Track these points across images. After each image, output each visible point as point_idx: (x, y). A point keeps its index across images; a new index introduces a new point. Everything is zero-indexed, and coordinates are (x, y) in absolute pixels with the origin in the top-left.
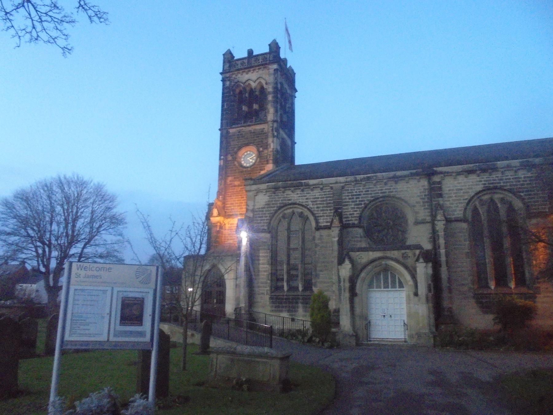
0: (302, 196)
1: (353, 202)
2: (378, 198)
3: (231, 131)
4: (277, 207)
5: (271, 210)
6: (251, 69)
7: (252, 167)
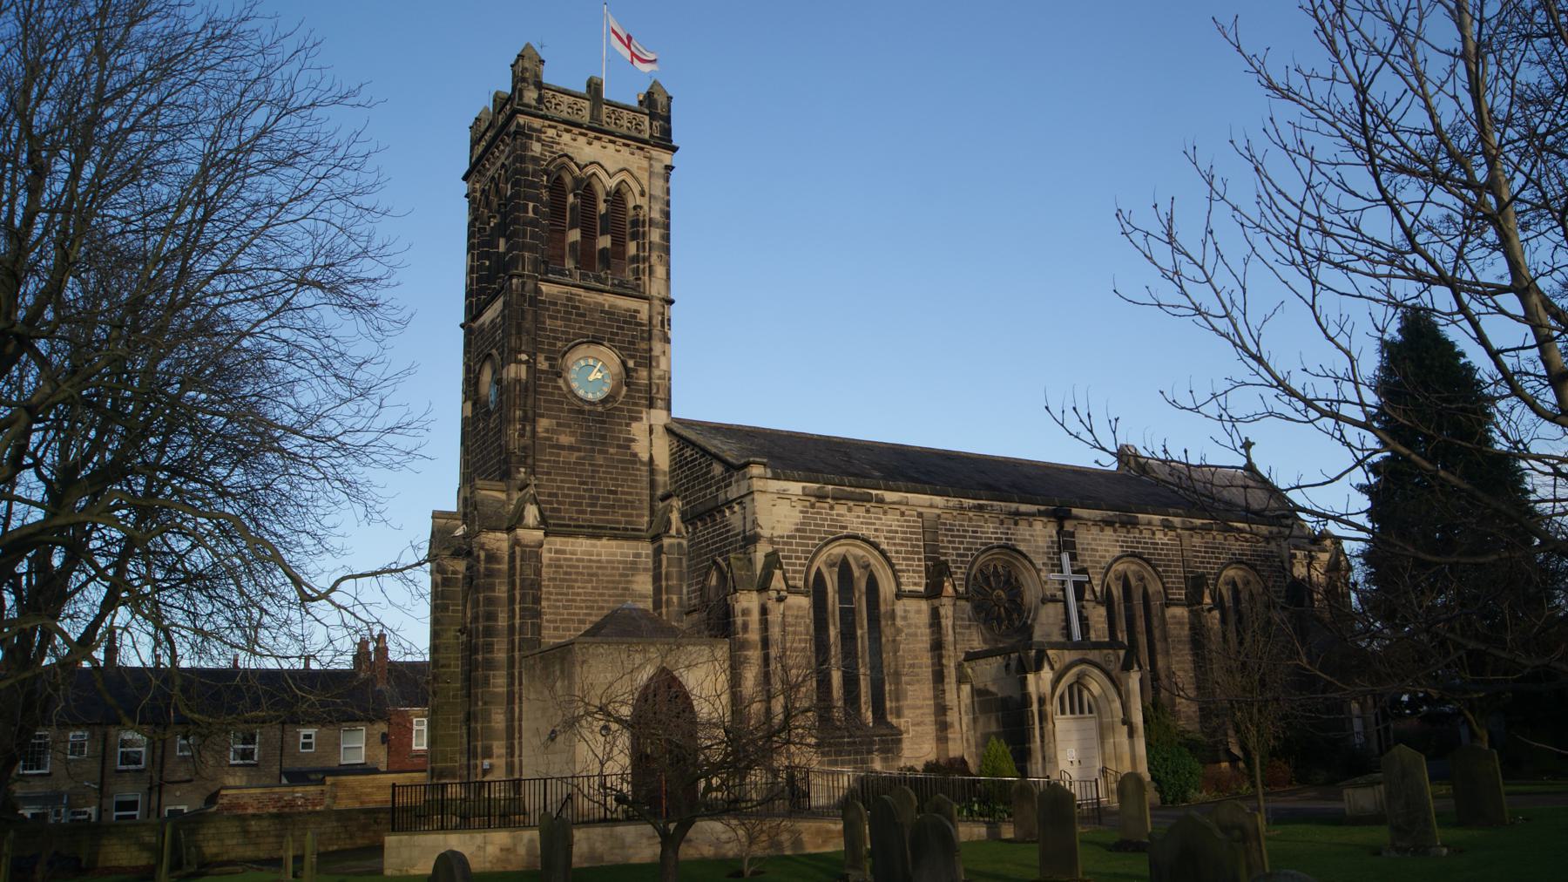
0: (867, 523)
1: (954, 548)
2: (993, 548)
3: (544, 287)
4: (821, 539)
5: (807, 545)
6: (606, 137)
7: (609, 406)
